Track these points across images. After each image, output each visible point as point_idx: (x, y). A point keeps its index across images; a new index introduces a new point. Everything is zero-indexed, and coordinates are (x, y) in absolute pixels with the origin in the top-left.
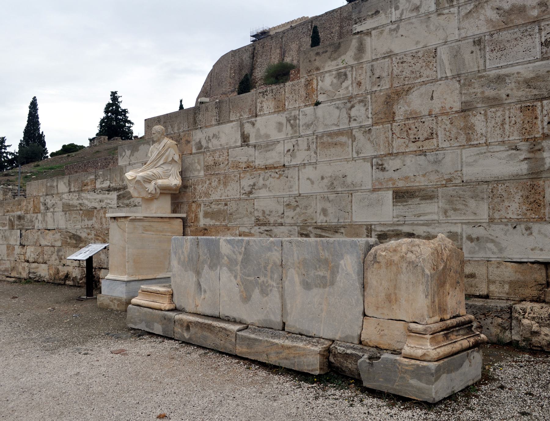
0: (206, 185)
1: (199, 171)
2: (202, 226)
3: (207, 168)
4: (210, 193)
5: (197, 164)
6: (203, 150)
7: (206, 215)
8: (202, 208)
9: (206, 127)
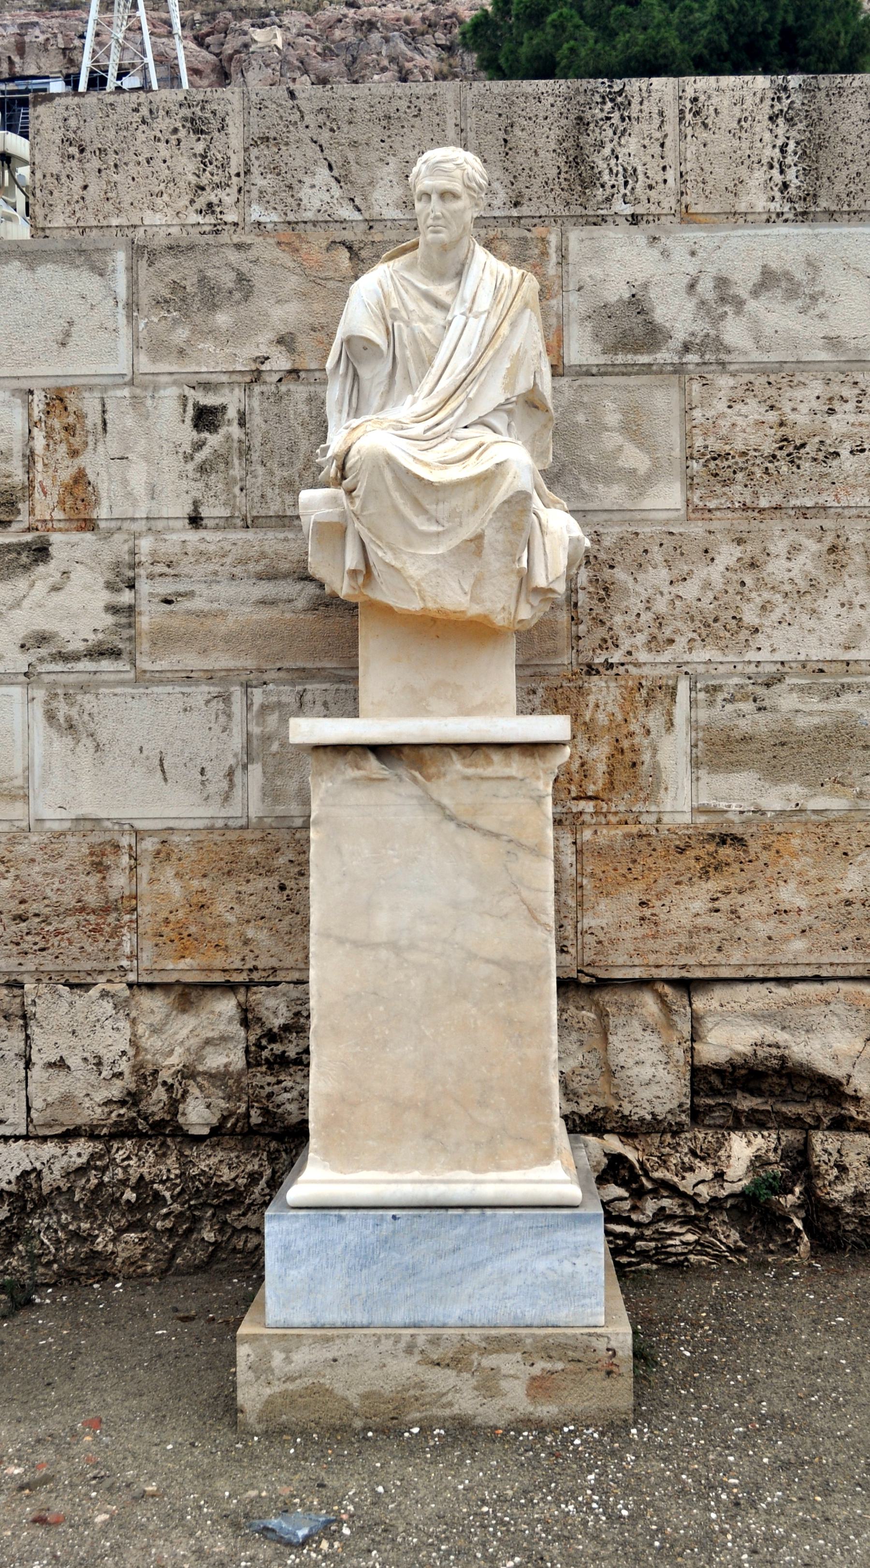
0: (716, 573)
1: (640, 483)
2: (687, 819)
3: (714, 466)
4: (750, 617)
5: (613, 440)
6: (665, 356)
7: (718, 751)
8: (681, 710)
9: (686, 216)
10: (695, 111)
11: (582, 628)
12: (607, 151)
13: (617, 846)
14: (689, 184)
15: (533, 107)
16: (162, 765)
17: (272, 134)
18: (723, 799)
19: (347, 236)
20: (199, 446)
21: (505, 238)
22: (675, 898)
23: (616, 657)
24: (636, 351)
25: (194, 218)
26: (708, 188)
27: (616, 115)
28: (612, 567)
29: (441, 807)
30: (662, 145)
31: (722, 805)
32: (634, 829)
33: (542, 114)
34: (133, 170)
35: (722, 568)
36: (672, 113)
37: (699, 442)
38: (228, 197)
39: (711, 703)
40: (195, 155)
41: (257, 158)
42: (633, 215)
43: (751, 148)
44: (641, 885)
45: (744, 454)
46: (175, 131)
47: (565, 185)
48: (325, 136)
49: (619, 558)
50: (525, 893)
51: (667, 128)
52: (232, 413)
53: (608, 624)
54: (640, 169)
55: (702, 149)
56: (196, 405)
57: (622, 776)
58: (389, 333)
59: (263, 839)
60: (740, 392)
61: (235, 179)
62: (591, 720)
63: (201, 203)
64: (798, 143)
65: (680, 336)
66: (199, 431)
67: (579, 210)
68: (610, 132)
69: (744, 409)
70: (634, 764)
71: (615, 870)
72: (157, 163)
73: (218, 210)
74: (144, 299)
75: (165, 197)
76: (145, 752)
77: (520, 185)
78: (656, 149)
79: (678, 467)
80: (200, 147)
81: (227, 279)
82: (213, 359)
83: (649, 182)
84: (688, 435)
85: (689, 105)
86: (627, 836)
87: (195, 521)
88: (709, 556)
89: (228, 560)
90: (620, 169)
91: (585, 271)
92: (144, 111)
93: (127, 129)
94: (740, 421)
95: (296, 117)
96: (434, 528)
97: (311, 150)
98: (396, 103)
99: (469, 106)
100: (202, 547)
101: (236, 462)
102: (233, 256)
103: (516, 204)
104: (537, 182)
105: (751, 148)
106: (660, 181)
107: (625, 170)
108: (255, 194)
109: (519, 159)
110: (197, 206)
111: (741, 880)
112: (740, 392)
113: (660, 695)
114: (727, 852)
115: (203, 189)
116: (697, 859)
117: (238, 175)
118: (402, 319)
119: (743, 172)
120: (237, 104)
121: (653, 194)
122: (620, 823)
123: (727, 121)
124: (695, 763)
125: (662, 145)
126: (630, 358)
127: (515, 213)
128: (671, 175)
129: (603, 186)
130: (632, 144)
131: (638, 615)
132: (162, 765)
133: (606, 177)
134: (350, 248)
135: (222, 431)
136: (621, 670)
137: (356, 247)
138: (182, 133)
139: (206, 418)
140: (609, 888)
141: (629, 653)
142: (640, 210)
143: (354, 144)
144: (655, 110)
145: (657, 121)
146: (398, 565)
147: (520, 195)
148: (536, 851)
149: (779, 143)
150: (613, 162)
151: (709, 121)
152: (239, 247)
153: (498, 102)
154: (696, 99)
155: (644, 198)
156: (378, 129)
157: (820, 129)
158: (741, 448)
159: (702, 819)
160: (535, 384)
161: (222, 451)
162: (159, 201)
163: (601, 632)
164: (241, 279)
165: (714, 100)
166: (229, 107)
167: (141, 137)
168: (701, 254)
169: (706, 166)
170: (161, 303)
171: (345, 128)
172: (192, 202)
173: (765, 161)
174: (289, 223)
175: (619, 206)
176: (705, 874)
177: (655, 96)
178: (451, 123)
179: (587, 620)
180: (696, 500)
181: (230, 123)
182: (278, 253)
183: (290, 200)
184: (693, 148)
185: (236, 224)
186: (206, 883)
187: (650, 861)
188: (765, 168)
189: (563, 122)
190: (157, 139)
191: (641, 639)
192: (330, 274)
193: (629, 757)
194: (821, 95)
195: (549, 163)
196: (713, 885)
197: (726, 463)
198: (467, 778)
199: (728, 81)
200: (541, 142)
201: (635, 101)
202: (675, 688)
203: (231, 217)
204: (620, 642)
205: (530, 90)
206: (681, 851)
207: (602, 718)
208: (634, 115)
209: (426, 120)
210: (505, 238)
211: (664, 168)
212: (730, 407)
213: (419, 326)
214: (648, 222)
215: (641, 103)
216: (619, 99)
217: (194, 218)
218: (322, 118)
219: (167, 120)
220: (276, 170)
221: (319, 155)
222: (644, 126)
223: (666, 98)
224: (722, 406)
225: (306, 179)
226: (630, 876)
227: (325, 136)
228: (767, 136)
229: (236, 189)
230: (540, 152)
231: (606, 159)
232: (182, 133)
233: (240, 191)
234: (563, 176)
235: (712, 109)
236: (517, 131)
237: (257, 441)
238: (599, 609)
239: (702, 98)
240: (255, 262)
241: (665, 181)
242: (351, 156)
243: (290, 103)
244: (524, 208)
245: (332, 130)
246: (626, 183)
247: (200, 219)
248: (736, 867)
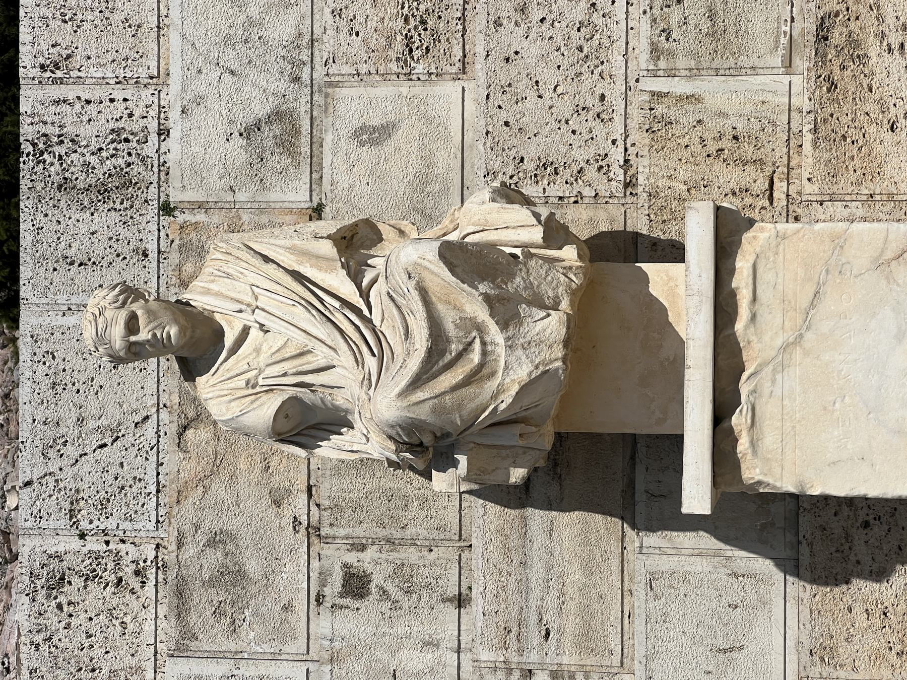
0: (532, 50)
2: (798, 81)
8: (678, 86)
10: (55, 67)
11: (588, 192)
12: (94, 160)
13: (826, 156)
15: (48, 236)
16: (725, 651)
17: (67, 505)
18: (777, 41)
19: (173, 429)
20: (384, 593)
21: (179, 267)
22: (887, 92)
23: (617, 155)
24: (297, 133)
25: (150, 588)
26: (134, 55)
27: (58, 150)
28: (522, 160)
29: (786, 348)
30: (88, 102)
31: (784, 40)
32: (808, 137)
33: (55, 227)
34: (98, 652)
35: (526, 43)
36: (57, 92)
37: (394, 67)
38: (129, 552)
39: (671, 54)
40: (85, 587)
41: (91, 522)
42: (159, 135)
43: (92, 10)
44: (872, 129)
45: (406, 20)
46: (60, 607)
47: (127, 204)
48: (71, 451)
49: (513, 153)
50: (889, 254)
51: (71, 97)
52: (351, 558)
53: (583, 164)
54: (112, 125)
55: (93, 61)
56: (342, 596)
57: (747, 150)
58: (270, 390)
59: (810, 545)
60: (343, 23)
61: (112, 546)
62: (685, 183)
63: (135, 583)
65: (283, 85)
66: (369, 593)
67: (153, 189)
68: (74, 156)
69: (360, 19)
70: (735, 138)
71: (853, 158)
72: (93, 627)
73: (142, 564)
74: (232, 645)
75: (127, 619)
76: (710, 669)
77: (126, 251)
78: (92, 109)
79: (418, 90)
80: (78, 582)
81: (214, 557)
82: (293, 577)
83: (125, 116)
84: (385, 77)
85: (48, 74)
86: (815, 144)
87: (461, 601)
88: (513, 56)
89: (504, 568)
90: (112, 146)
91: (214, 185)
92: (39, 638)
93: (56, 657)
94: (372, 24)
95: (50, 480)
96: (477, 346)
97: (86, 465)
98: (40, 377)
99: (44, 301)
100: (490, 595)
101: (402, 555)
102: (190, 551)
103: (146, 255)
104: (124, 233)
105: (92, 10)
106: (124, 105)
107: (113, 141)
108: (127, 525)
109: (99, 250)
110: (137, 586)
111: (868, 19)
112: (343, 23)
113: (660, 110)
114: (837, 36)
115: (120, 580)
116: (843, 68)
117: (107, 543)
118: (257, 377)
120: (37, 541)
121: (137, 113)
122: (800, 154)
123: (64, 35)
124: (738, 71)
125: (88, 102)
126: (305, 139)
127: (153, 255)
128: (118, 95)
129: (129, 165)
130: (87, 131)
131: (574, 132)
132: (725, 651)
133: (120, 162)
134: (185, 428)
135: (369, 568)
136: (631, 150)
137: (184, 422)
138: (62, 599)
139: (356, 585)
140: (874, 165)
141: (614, 142)
142: (153, 126)
143: (80, 420)
144: (53, 108)
145: (65, 108)
146: (515, 389)
147: (136, 251)
148: (838, 243)
150: (104, 154)
151: (65, 53)
152: (180, 545)
153: (42, 270)
154: (42, 67)
155: (143, 122)
156: (66, 396)
158: (400, 22)
159: (799, 63)
160: (329, 237)
161: (390, 570)
162: (131, 627)
163: (591, 173)
164: (213, 542)
165: (44, 46)
166: (37, 550)
167: (66, 642)
168: (200, 62)
170: (234, 629)
171: (63, 430)
172: (132, 592)
174: (158, 491)
175: (149, 150)
176: (863, 59)
177: (38, 109)
178: (61, 321)
179: (578, 187)
180: (454, 70)
181: (55, 549)
182: (188, 504)
183: (134, 489)
184: (92, 70)
185: (158, 546)
186: (858, 609)
187: (844, 120)
189: (62, 204)
190: (68, 626)
191: (599, 129)
192: (210, 450)
193: (727, 143)
195: (105, 220)
196: (873, 49)
197: (416, 38)
198: (753, 317)
199: (24, 35)
200: (83, 228)
201: (43, 129)
202: (653, 94)
203: (150, 552)
204: (602, 152)
205: (29, 239)
206: (833, 86)
207: (683, 173)
208: (57, 131)
209: (57, 347)
210: (179, 267)
211: (112, 101)
212: (357, 34)
213: (263, 359)
214: (166, 119)
215: (45, 123)
216: (41, 146)
217: (150, 588)
218: (52, 453)
219: (49, 615)
220: (104, 504)
222: (67, 121)
223: (40, 97)
224: (357, 42)
225: (114, 470)
226: (861, 143)
227: (71, 451)
229: (121, 546)
230: (93, 229)
231: (102, 162)
232: (62, 599)
233: (123, 541)
234: (118, 207)
235: (51, 50)
236: (70, 253)
237: (382, 533)
238: (567, 174)
239: (41, 60)
240: (197, 527)
241: (125, 100)
242: (91, 424)
243: (35, 485)
244: (149, 246)
245: (65, 443)
246: (127, 140)
247: (151, 584)
248: (853, 25)
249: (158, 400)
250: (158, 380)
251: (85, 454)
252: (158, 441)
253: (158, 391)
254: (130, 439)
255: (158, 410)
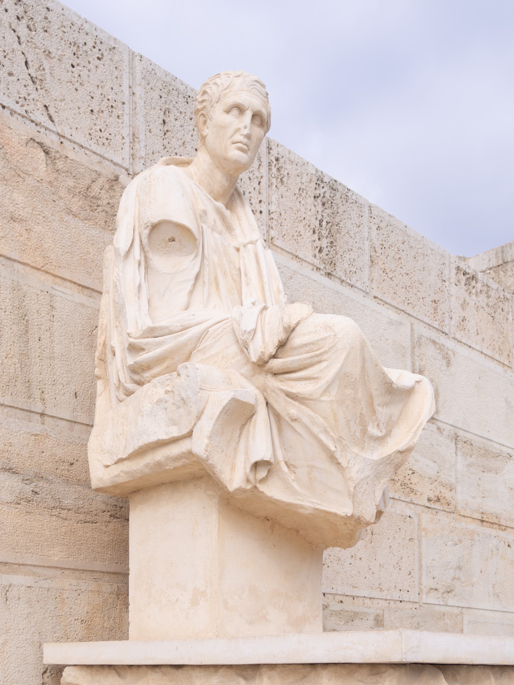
14: (275, 223)
43: (305, 213)
48: (22, 31)
64: (328, 223)
106: (259, 211)
119: (301, 229)
149: (320, 217)
157: (337, 220)
169: (283, 213)
173: (312, 226)
188: (312, 231)
194: (338, 195)
221: (16, 45)
228: (313, 209)
242: (46, 65)
249: (67, 138)
250: (82, 146)
251: (20, 43)
252: (32, 121)
253: (75, 143)
254: (34, 95)
255: (59, 134)
